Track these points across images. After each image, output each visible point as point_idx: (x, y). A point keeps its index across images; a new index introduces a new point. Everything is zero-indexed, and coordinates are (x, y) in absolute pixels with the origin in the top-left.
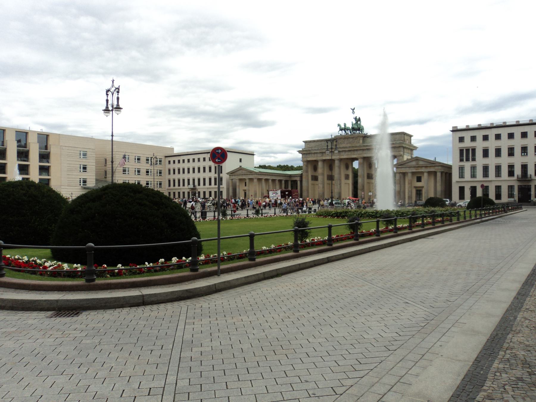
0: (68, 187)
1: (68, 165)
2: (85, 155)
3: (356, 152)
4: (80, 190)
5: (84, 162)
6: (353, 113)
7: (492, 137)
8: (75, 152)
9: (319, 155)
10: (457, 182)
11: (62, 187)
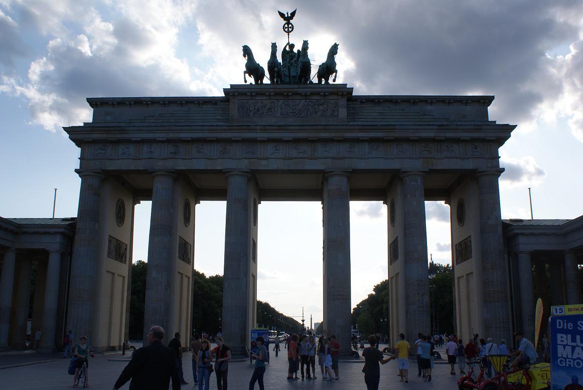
3: (320, 150)
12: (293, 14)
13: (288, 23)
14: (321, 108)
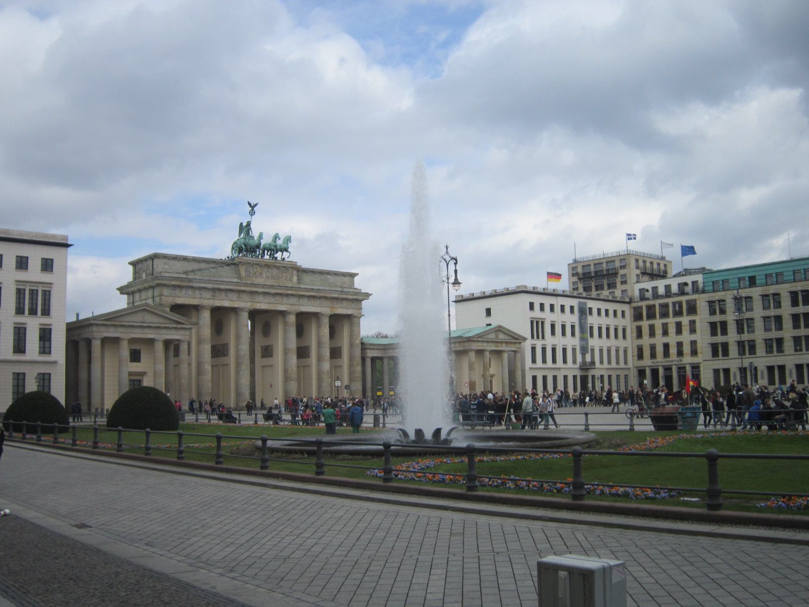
3: (285, 300)
6: (252, 213)
7: (557, 309)
9: (208, 295)
10: (531, 368)
12: (256, 205)
13: (253, 210)
14: (285, 275)
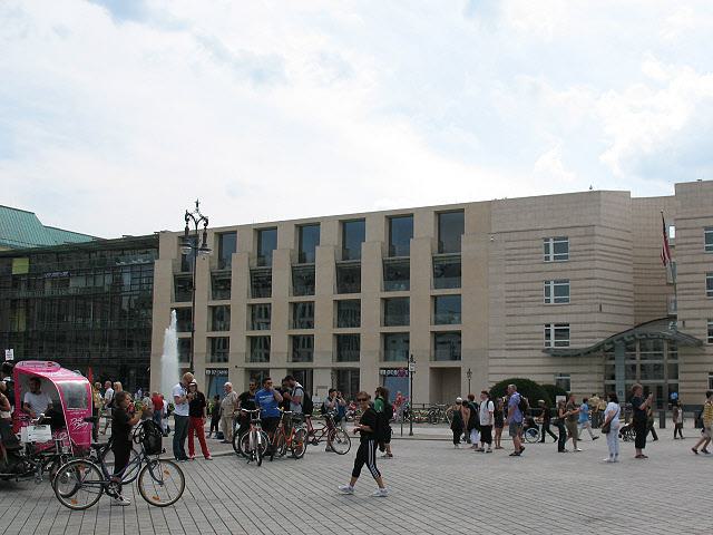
0: (508, 354)
1: (512, 287)
2: (561, 247)
4: (547, 361)
5: (556, 271)
8: (530, 244)
11: (492, 353)
